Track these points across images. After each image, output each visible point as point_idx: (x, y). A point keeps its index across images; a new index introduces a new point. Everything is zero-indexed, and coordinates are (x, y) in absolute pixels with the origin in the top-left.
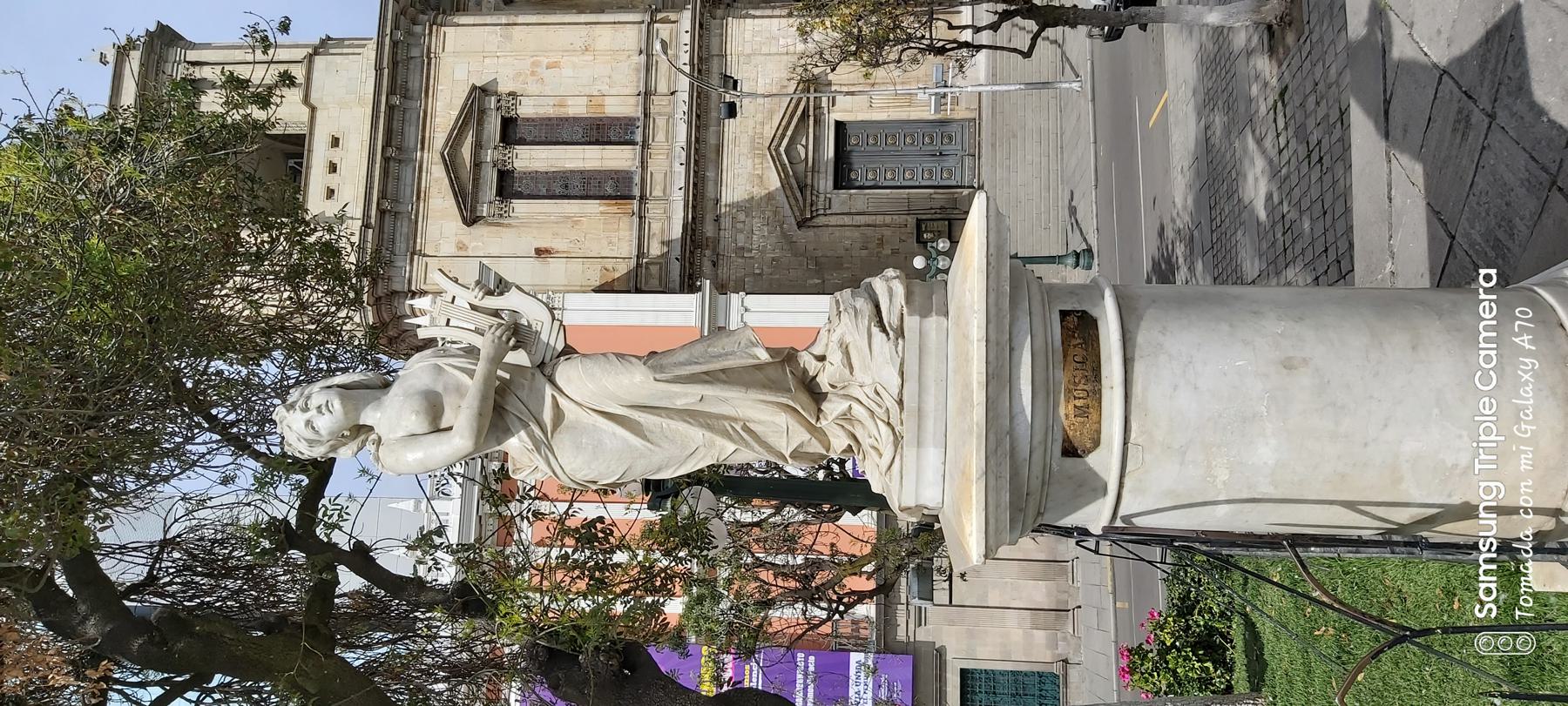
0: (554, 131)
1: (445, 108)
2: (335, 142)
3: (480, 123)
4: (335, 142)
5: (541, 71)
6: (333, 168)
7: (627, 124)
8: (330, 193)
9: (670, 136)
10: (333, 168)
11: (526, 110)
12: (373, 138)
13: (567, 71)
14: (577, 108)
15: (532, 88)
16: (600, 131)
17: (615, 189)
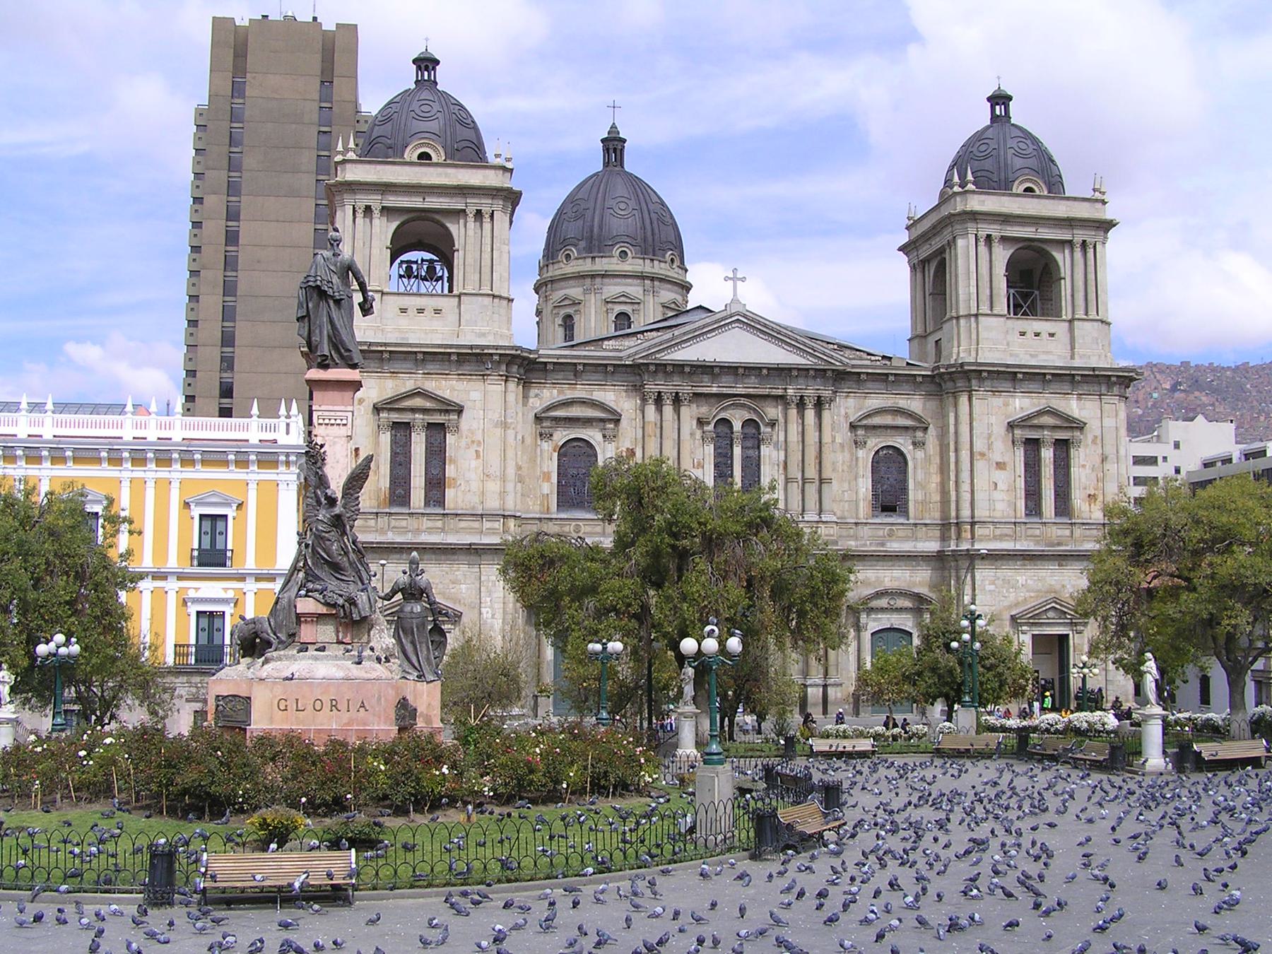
0: (437, 454)
1: (448, 387)
2: (438, 311)
3: (440, 411)
4: (438, 311)
5: (475, 447)
6: (421, 311)
7: (441, 502)
8: (403, 310)
9: (430, 530)
10: (421, 311)
11: (450, 439)
12: (427, 346)
13: (474, 463)
14: (450, 471)
15: (463, 443)
16: (436, 485)
17: (399, 493)
